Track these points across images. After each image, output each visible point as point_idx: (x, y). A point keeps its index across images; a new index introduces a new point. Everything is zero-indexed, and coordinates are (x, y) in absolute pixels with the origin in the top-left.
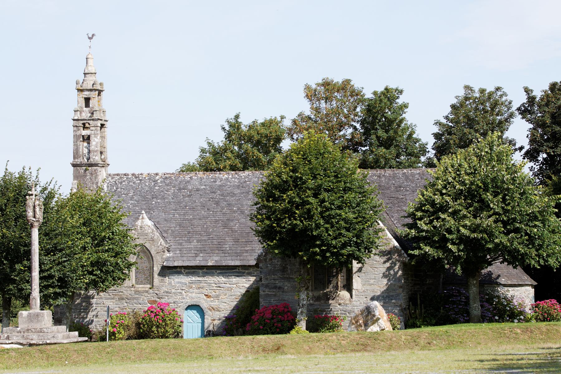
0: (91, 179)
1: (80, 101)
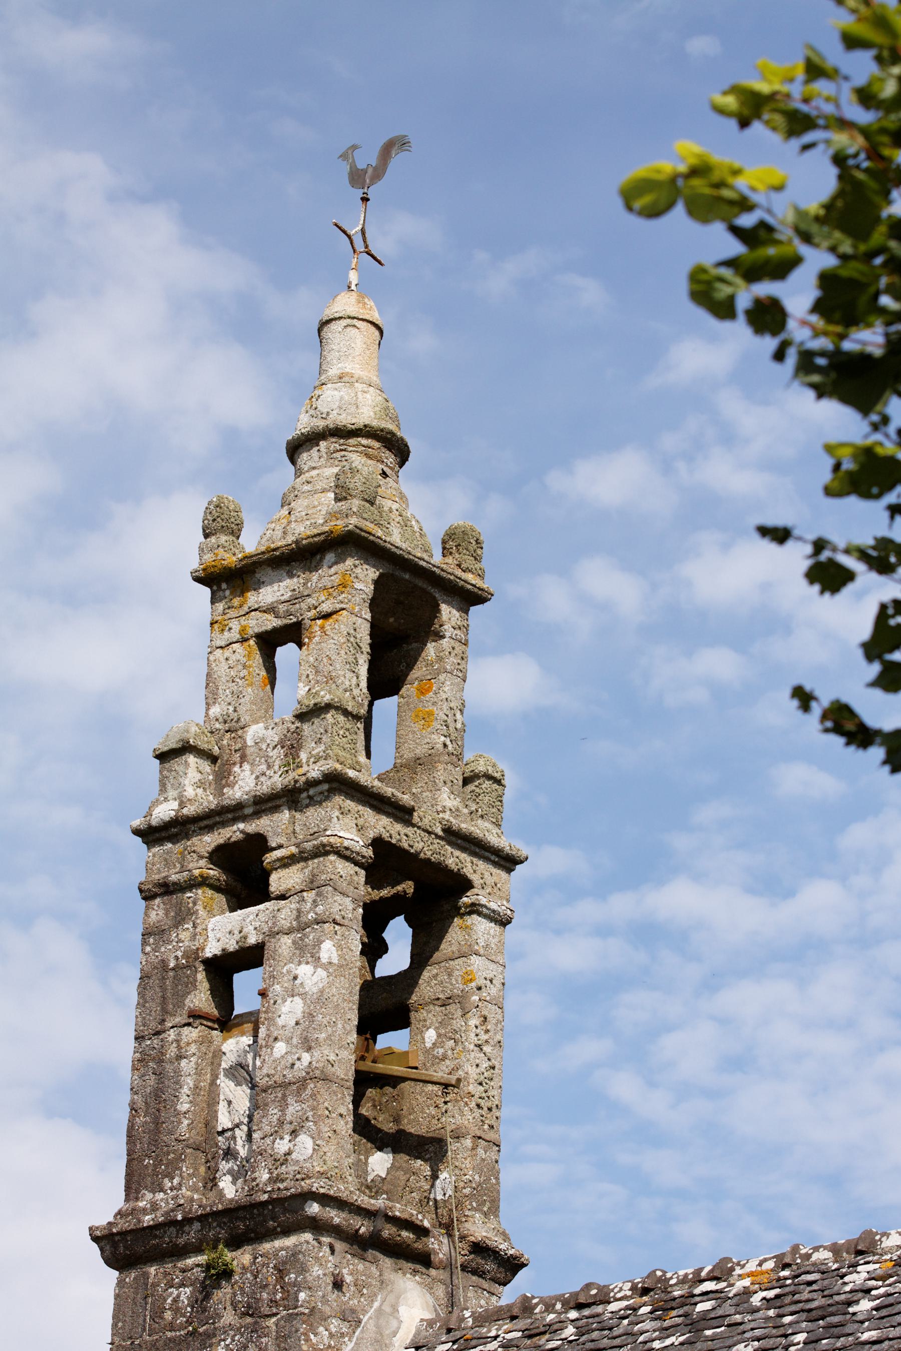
1: (222, 670)
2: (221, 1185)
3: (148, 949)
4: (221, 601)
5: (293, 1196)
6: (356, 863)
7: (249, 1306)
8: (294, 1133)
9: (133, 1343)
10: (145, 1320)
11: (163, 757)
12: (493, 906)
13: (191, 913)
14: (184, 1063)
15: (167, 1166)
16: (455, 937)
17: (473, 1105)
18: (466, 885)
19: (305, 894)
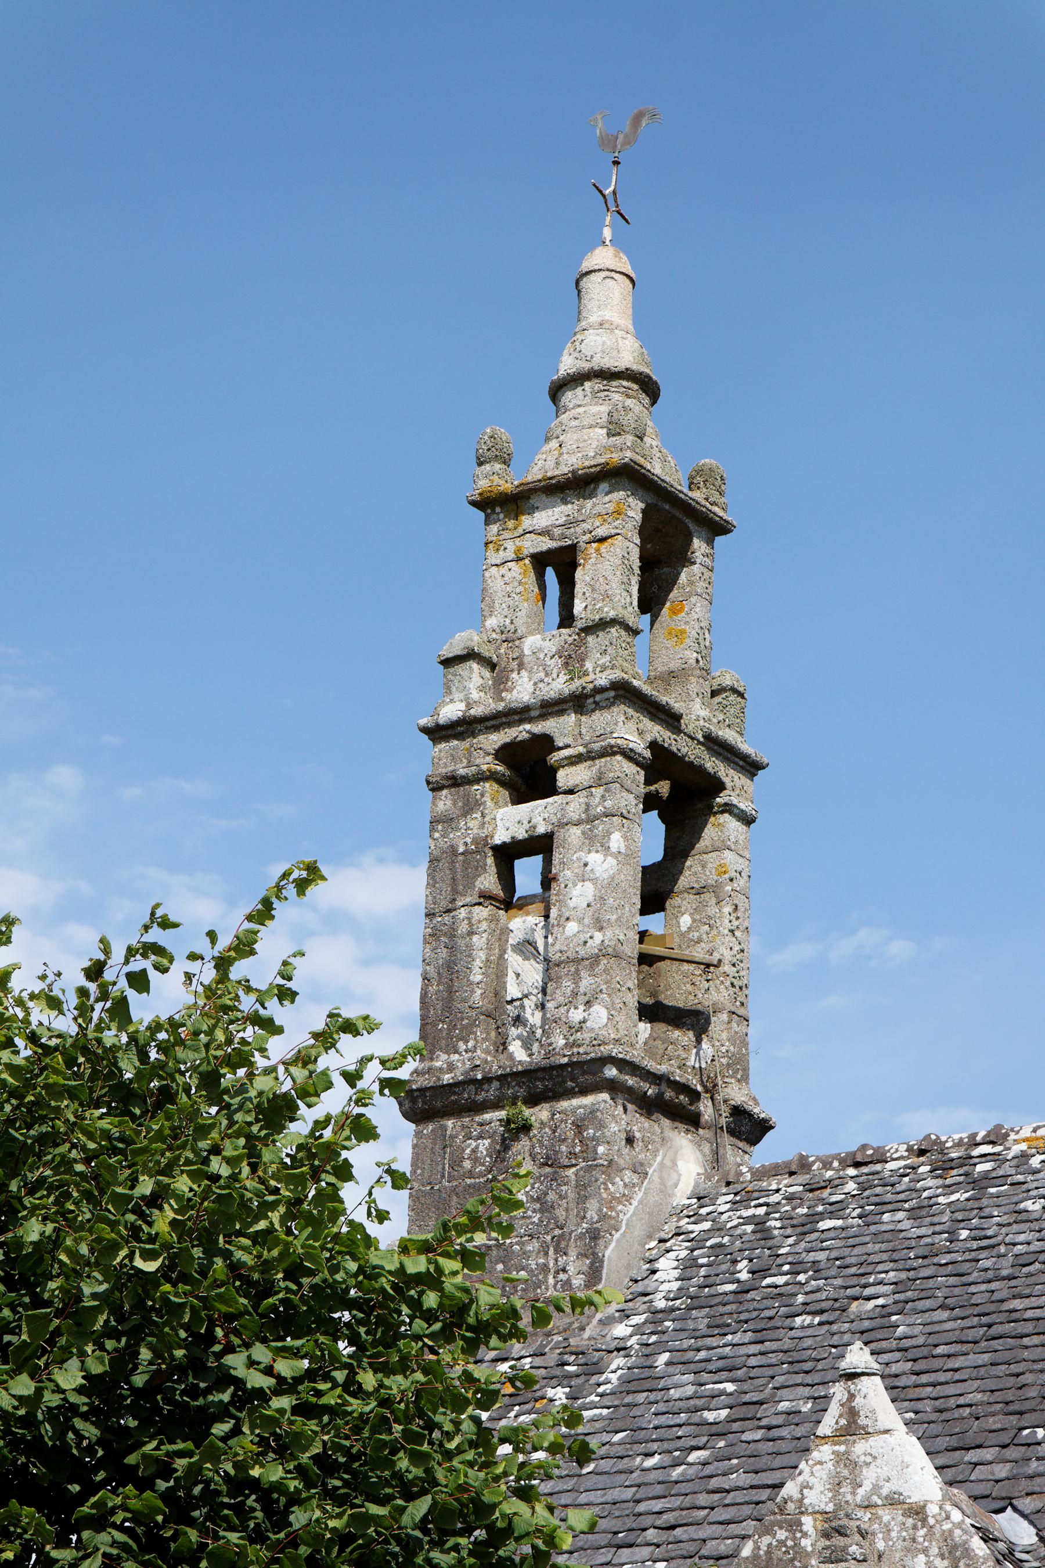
0: (546, 1208)
2: (511, 1048)
3: (437, 835)
4: (495, 523)
5: (593, 1060)
6: (638, 764)
7: (548, 1158)
8: (588, 1003)
9: (432, 1188)
10: (444, 1168)
11: (447, 663)
12: (742, 806)
13: (478, 804)
14: (475, 938)
15: (461, 1030)
16: (710, 833)
17: (728, 983)
18: (718, 786)
19: (593, 790)
